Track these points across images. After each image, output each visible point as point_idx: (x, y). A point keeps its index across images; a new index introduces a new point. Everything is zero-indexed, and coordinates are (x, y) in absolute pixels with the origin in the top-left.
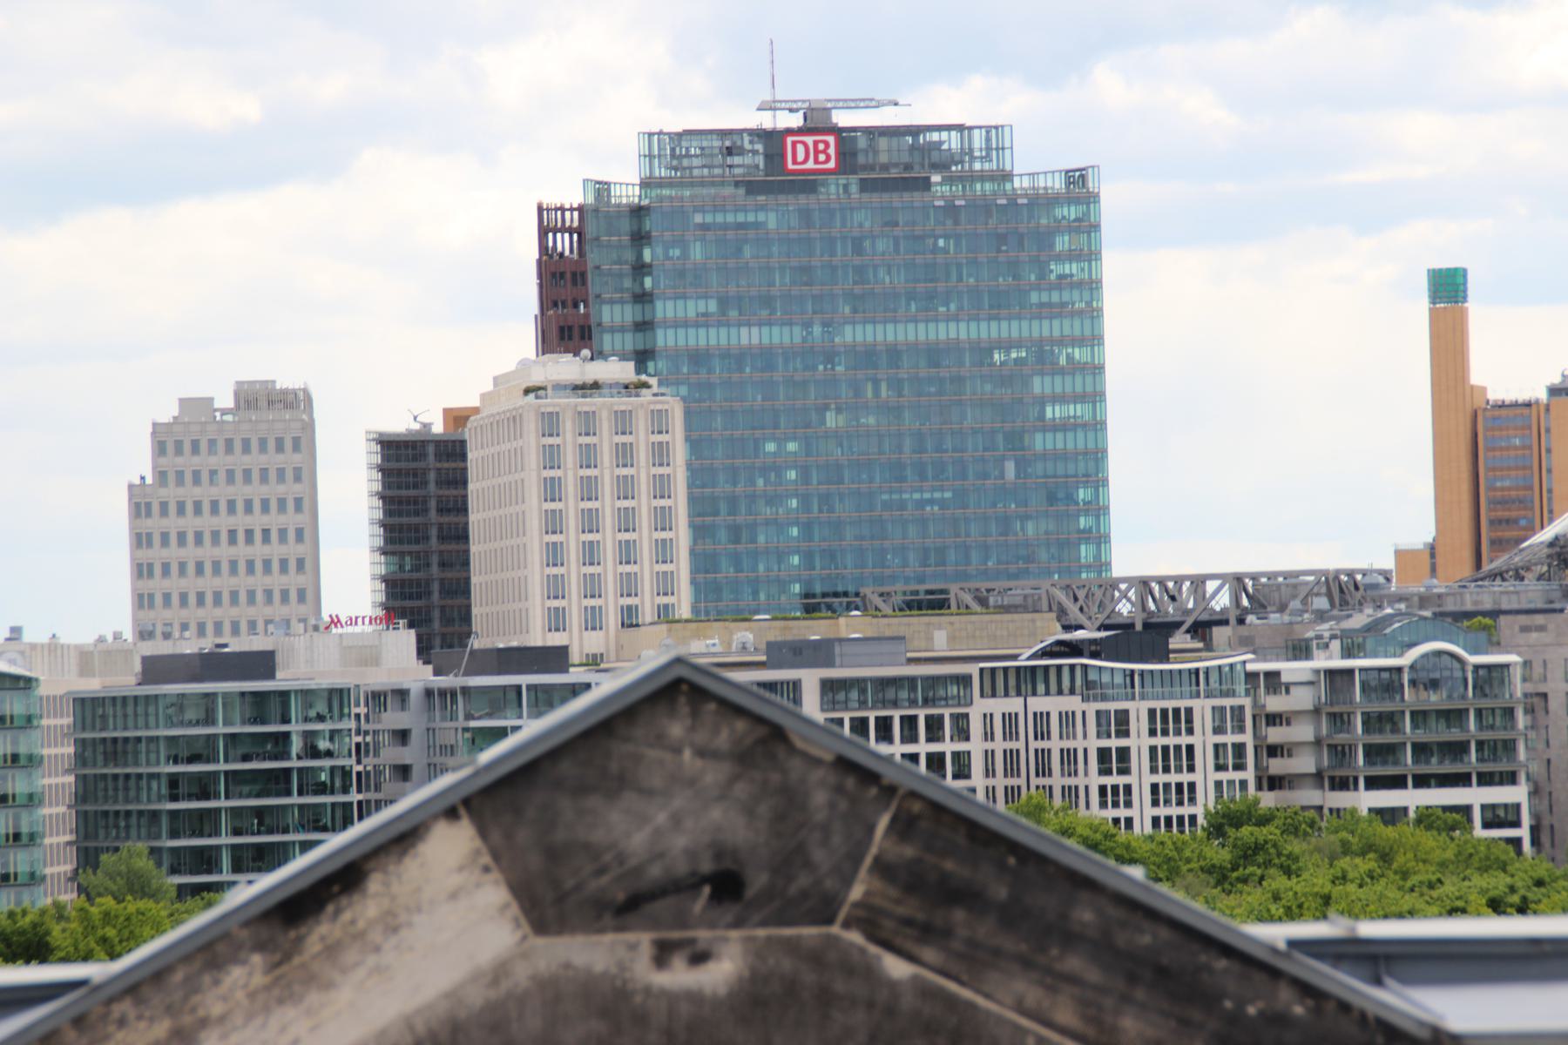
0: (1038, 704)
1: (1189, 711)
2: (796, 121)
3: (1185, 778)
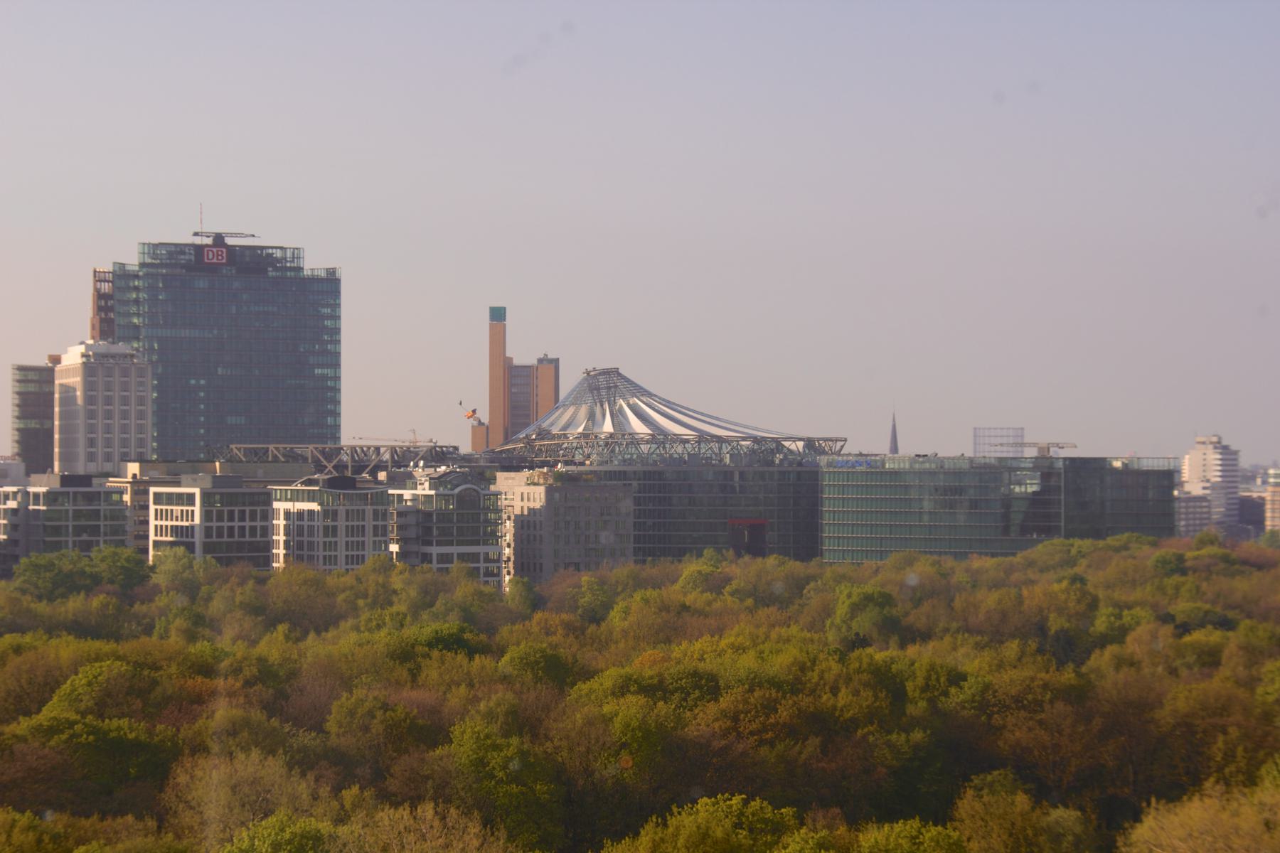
1: (364, 511)
2: (209, 241)
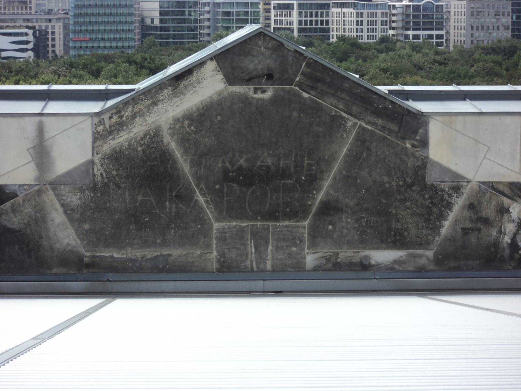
0: (344, 10)
1: (376, 13)
3: (374, 27)
